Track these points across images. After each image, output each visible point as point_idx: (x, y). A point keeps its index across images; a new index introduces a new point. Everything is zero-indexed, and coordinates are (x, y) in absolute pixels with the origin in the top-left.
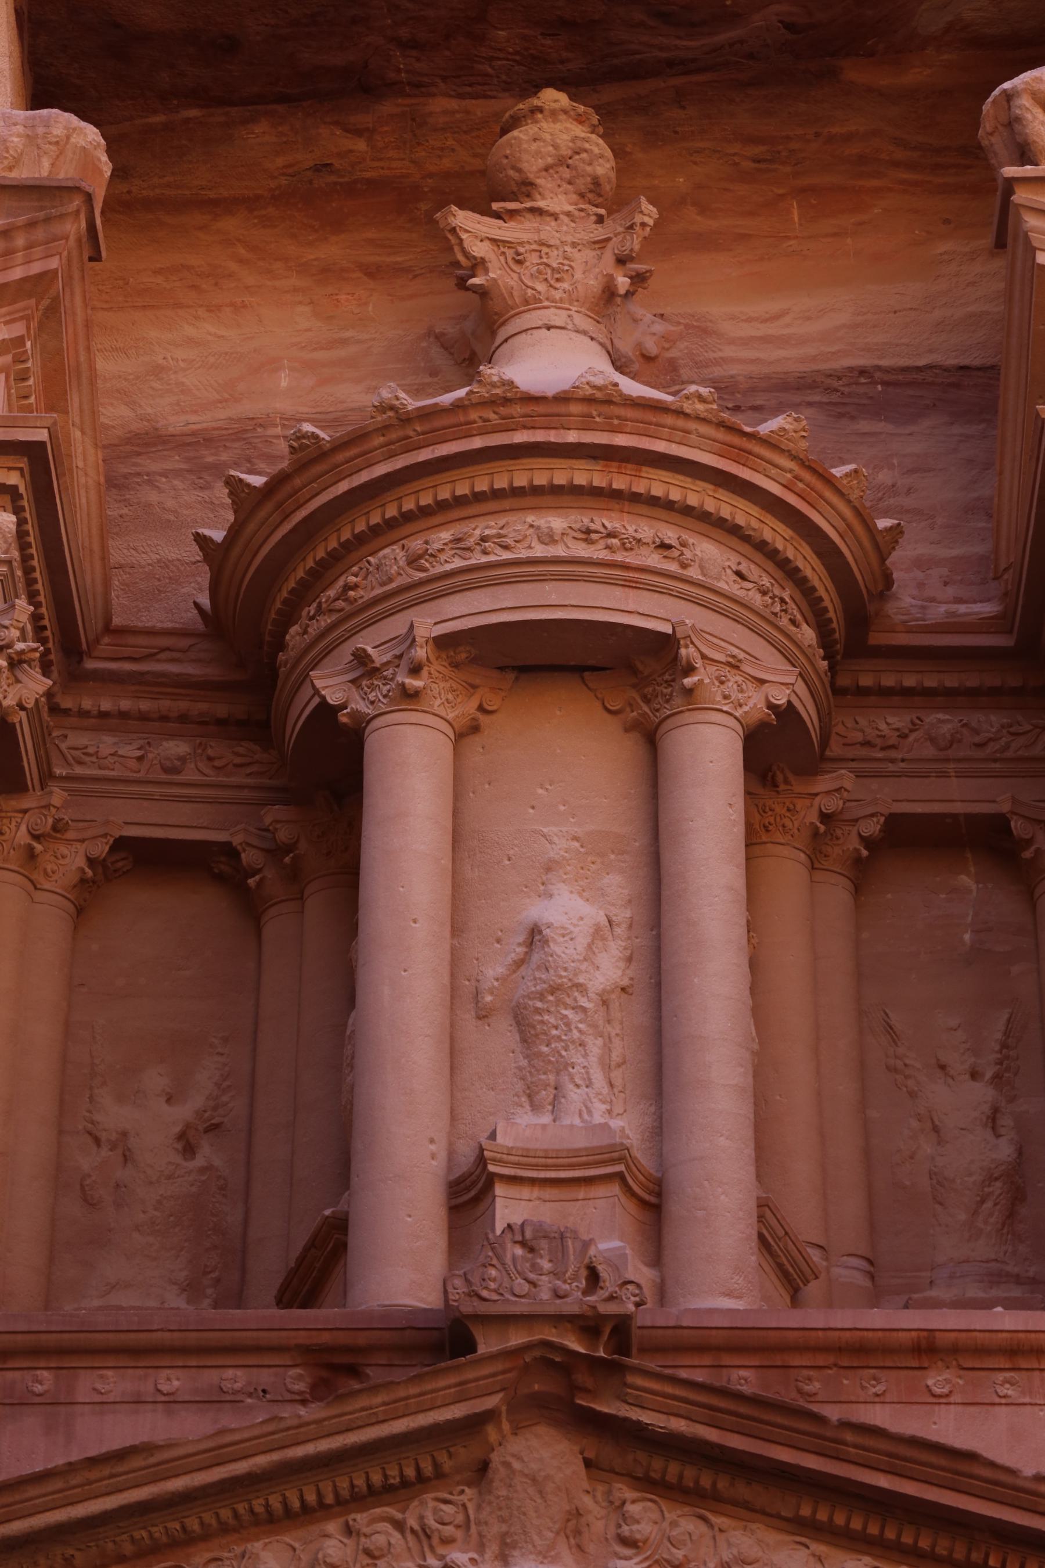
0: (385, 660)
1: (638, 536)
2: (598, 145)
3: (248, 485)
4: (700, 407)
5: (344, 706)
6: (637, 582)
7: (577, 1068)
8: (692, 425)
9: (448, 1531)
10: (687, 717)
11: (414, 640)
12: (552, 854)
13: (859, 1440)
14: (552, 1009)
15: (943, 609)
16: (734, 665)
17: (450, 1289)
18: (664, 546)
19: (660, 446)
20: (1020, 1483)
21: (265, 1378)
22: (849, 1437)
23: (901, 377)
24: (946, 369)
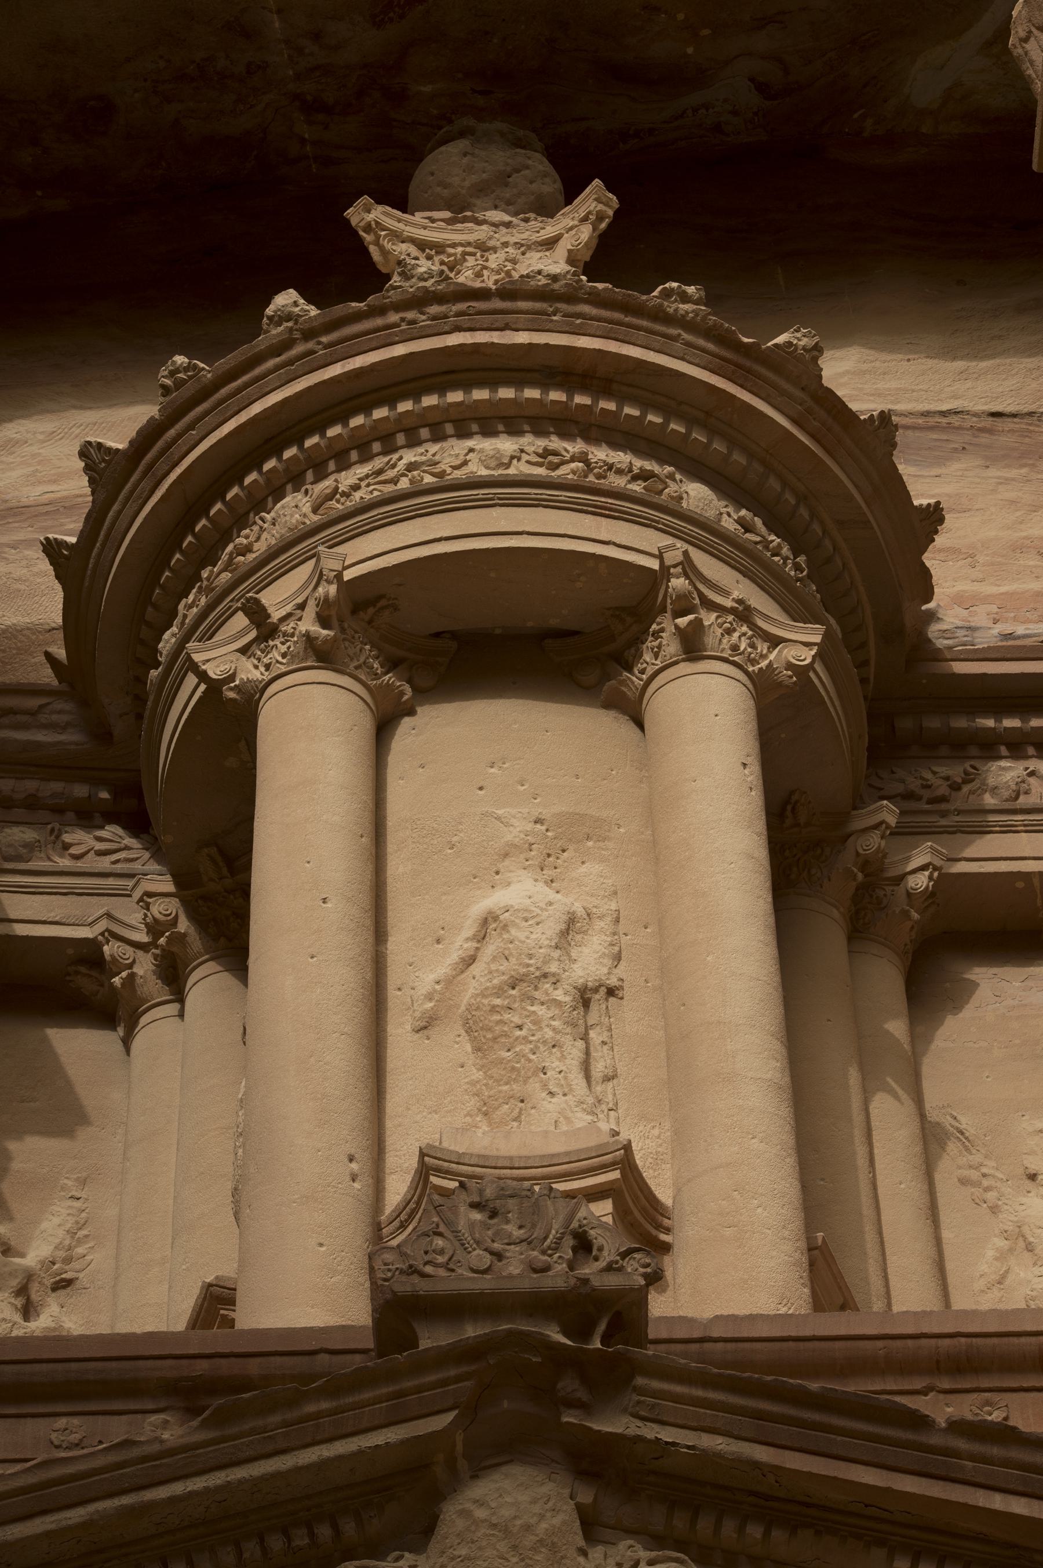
0: (284, 613)
1: (610, 461)
2: (539, 163)
3: (109, 450)
5: (232, 678)
6: (610, 510)
7: (549, 1074)
8: (673, 331)
10: (684, 668)
11: (321, 574)
12: (509, 837)
13: (976, 1448)
14: (516, 1005)
15: (995, 632)
17: (378, 1264)
18: (644, 476)
22: (962, 1444)
23: (920, 421)
24: (976, 415)
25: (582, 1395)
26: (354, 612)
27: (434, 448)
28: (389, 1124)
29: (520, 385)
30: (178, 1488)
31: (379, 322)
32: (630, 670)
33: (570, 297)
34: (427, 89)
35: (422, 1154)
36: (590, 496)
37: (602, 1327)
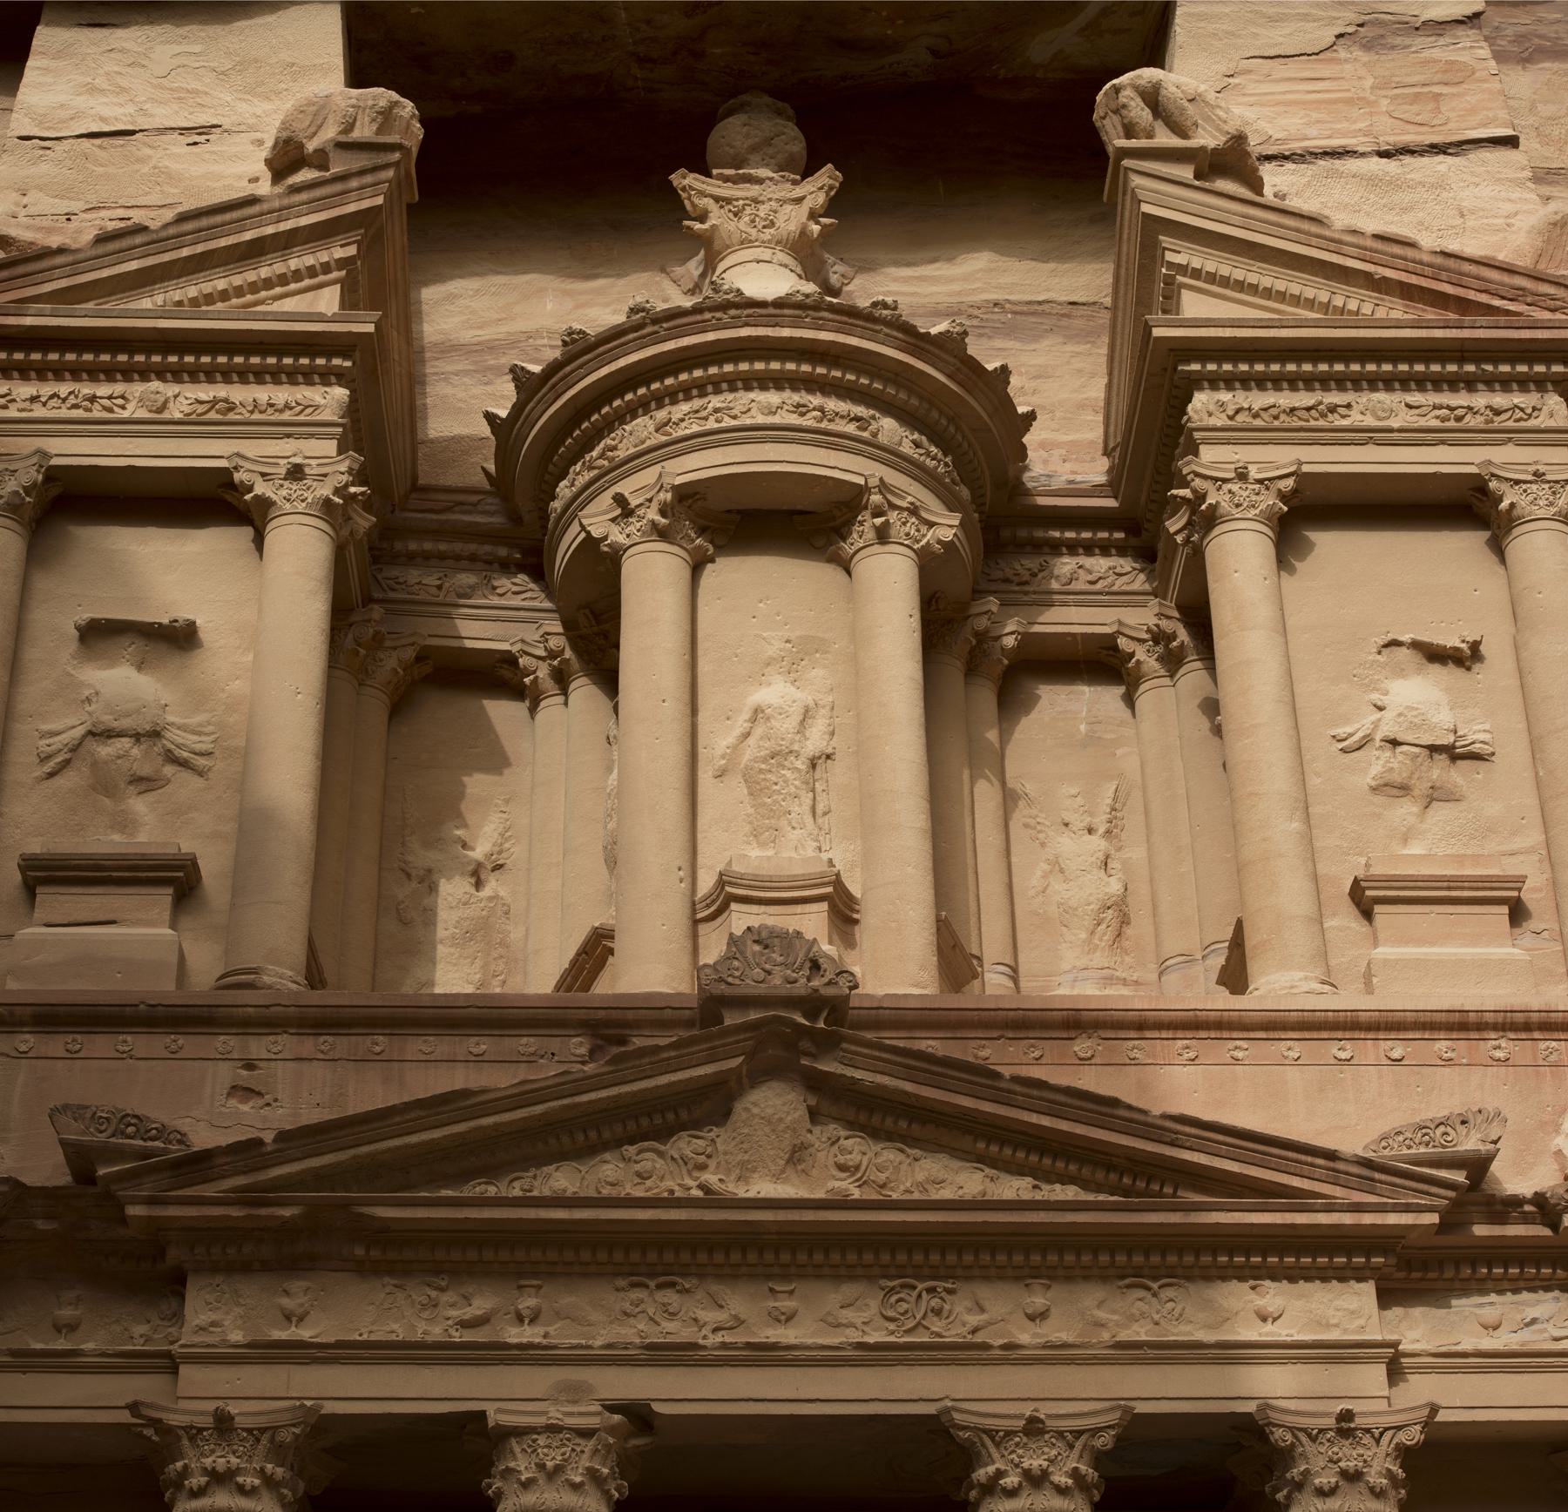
2: (792, 130)
3: (528, 372)
4: (885, 312)
5: (606, 538)
9: (702, 1158)
10: (877, 548)
12: (770, 653)
16: (914, 511)
18: (857, 419)
19: (854, 341)
20: (1150, 1120)
21: (554, 1044)
22: (1018, 1088)
25: (813, 1050)
26: (680, 501)
27: (730, 396)
28: (699, 836)
29: (783, 360)
30: (593, 1096)
31: (699, 317)
32: (844, 539)
33: (817, 307)
34: (719, 51)
35: (721, 874)
37: (825, 1014)
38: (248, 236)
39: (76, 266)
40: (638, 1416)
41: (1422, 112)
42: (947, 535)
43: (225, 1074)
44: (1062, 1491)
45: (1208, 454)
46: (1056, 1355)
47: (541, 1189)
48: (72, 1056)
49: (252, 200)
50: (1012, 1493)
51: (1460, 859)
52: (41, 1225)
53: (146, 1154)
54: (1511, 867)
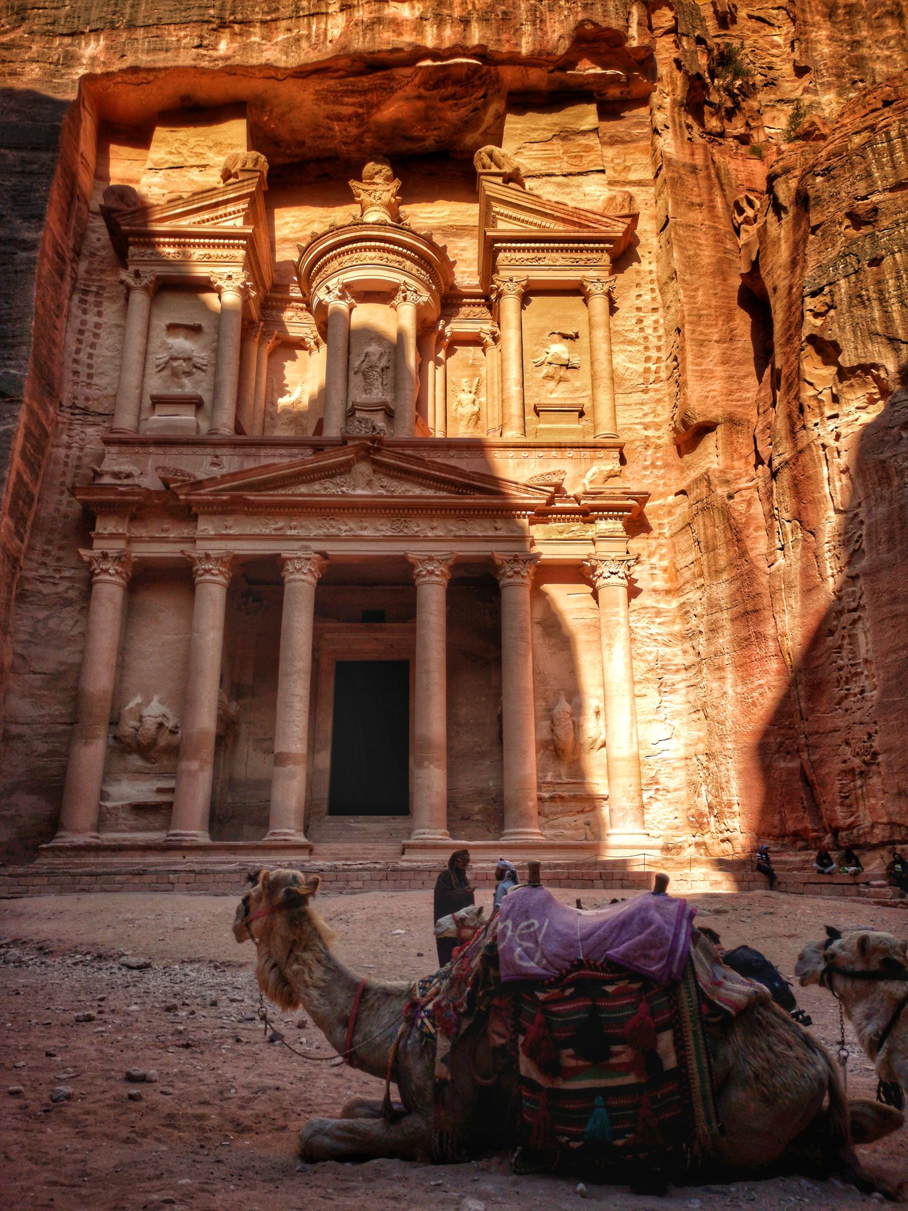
2: (388, 168)
16: (416, 292)
19: (397, 236)
21: (303, 451)
36: (388, 267)
38: (214, 201)
39: (163, 210)
40: (324, 555)
41: (576, 161)
42: (425, 299)
43: (210, 459)
44: (437, 576)
45: (502, 273)
46: (438, 539)
47: (297, 492)
48: (165, 454)
49: (215, 189)
50: (424, 576)
51: (565, 399)
52: (156, 501)
53: (184, 481)
54: (581, 401)
